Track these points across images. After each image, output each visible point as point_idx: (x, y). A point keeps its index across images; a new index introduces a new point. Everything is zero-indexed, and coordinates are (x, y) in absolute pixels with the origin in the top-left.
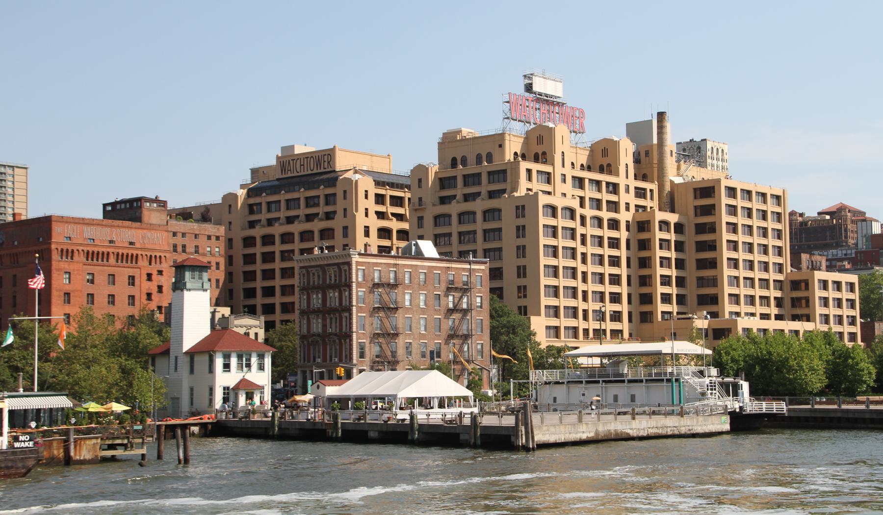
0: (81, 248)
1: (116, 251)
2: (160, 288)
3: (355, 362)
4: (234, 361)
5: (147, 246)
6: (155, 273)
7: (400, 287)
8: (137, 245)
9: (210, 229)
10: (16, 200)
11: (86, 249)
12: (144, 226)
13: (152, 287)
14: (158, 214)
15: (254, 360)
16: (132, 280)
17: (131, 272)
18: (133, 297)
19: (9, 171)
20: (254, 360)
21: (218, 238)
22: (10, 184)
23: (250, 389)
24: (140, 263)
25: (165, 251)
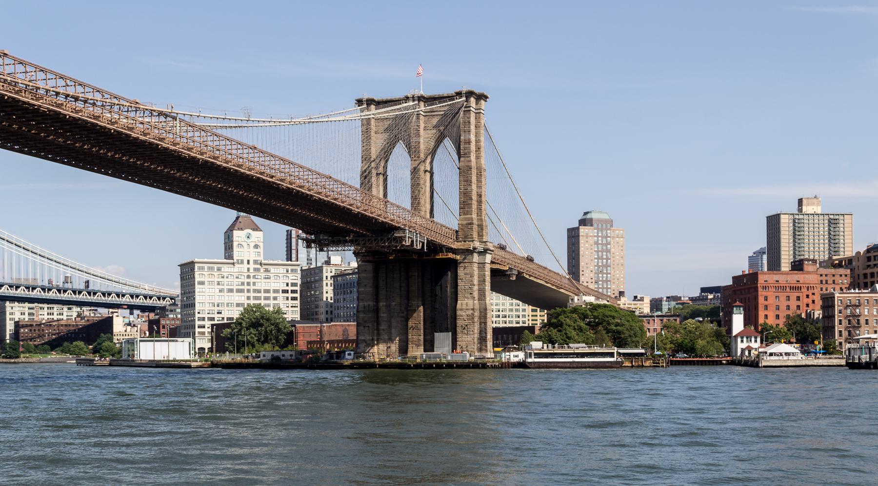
0: (772, 285)
1: (790, 285)
2: (813, 302)
3: (836, 338)
4: (745, 339)
5: (806, 282)
6: (810, 294)
7: (862, 306)
8: (801, 282)
9: (841, 271)
10: (845, 234)
11: (774, 285)
12: (804, 272)
13: (810, 301)
14: (812, 266)
15: (753, 339)
16: (798, 298)
17: (798, 294)
18: (799, 306)
19: (841, 217)
20: (753, 339)
21: (846, 275)
22: (842, 225)
23: (749, 349)
24: (802, 290)
25: (816, 284)
